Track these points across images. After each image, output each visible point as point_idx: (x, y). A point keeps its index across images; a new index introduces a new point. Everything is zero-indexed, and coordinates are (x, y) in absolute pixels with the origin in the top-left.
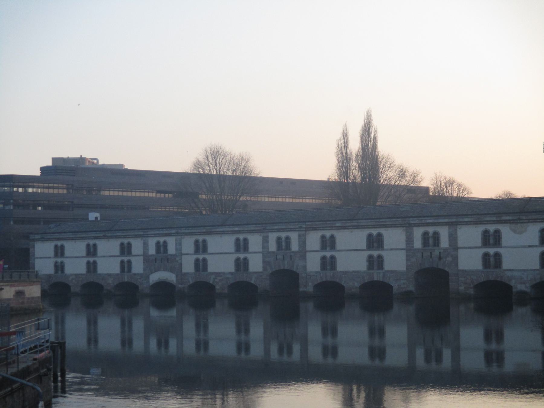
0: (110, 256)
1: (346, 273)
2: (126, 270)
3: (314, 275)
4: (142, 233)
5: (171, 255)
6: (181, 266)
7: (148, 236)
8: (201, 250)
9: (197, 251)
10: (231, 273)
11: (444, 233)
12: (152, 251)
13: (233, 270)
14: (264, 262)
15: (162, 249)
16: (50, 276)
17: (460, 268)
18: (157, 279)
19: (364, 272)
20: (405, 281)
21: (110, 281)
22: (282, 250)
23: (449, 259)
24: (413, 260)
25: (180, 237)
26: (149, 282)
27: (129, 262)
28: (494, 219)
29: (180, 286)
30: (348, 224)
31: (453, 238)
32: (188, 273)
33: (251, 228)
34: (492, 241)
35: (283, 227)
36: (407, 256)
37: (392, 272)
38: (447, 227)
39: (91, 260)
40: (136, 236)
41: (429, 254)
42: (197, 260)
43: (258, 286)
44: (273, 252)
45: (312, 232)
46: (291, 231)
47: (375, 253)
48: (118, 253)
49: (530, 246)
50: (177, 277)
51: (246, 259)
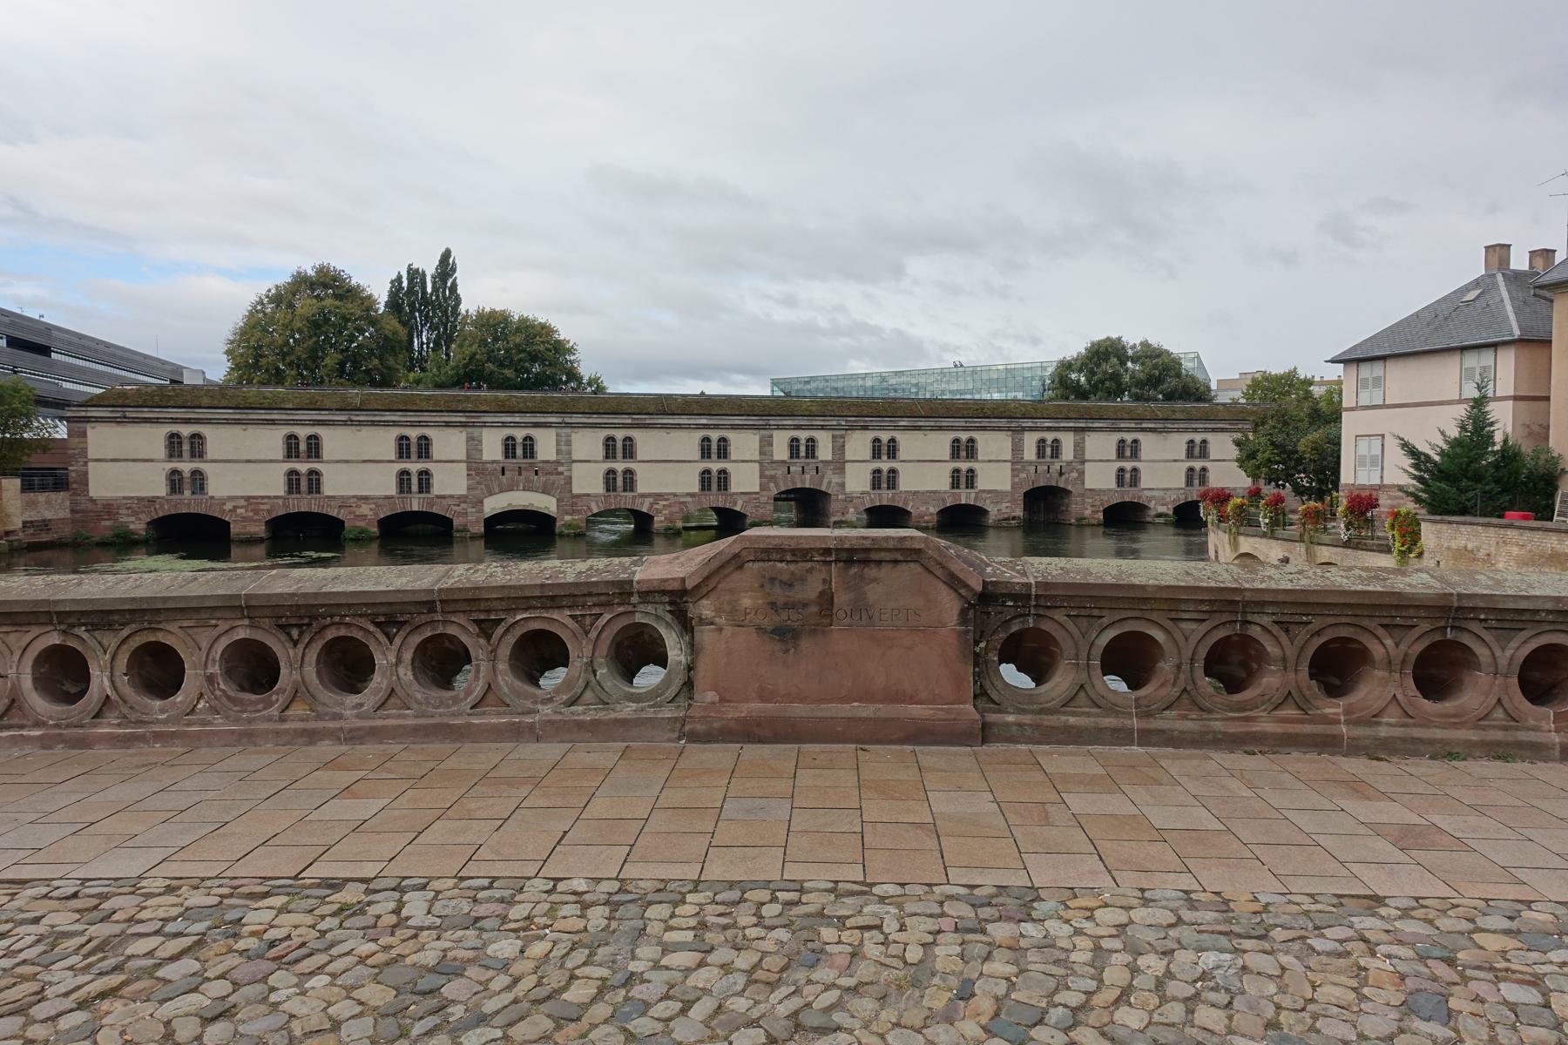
0: (364, 461)
1: (916, 492)
4: (464, 419)
5: (547, 462)
7: (484, 425)
10: (692, 495)
11: (1068, 441)
13: (696, 489)
14: (762, 476)
15: (519, 451)
16: (152, 500)
17: (1088, 485)
19: (945, 492)
20: (1009, 504)
21: (365, 510)
22: (798, 457)
23: (1075, 475)
26: (482, 511)
28: (1133, 425)
29: (568, 518)
30: (920, 424)
31: (1079, 448)
32: (588, 495)
34: (1128, 453)
36: (1013, 470)
37: (989, 492)
40: (448, 425)
41: (1046, 468)
42: (611, 473)
44: (783, 462)
50: (558, 501)
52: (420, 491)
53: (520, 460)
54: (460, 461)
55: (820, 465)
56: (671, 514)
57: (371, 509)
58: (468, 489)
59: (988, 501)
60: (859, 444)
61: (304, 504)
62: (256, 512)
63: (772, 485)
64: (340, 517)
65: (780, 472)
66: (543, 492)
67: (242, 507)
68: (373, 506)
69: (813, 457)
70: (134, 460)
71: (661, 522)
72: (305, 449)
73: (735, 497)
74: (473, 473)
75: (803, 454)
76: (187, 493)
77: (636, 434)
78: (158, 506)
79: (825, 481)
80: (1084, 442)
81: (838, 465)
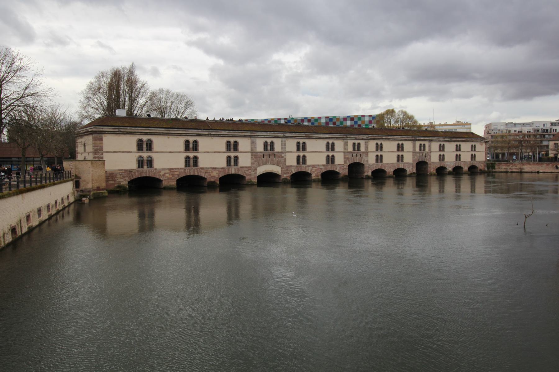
0: (215, 152)
1: (388, 164)
2: (232, 163)
3: (372, 166)
5: (278, 152)
7: (258, 137)
8: (301, 149)
10: (324, 165)
13: (324, 162)
14: (345, 158)
15: (269, 148)
16: (131, 171)
17: (432, 161)
18: (264, 171)
19: (396, 164)
23: (429, 157)
24: (416, 157)
25: (285, 139)
26: (256, 173)
29: (285, 176)
31: (430, 147)
32: (291, 166)
34: (442, 149)
36: (413, 155)
38: (428, 142)
40: (245, 136)
43: (340, 173)
44: (351, 152)
46: (363, 139)
48: (224, 149)
49: (453, 152)
51: (333, 156)
52: (234, 165)
53: (269, 152)
54: (248, 152)
55: (361, 153)
56: (317, 173)
57: (217, 173)
58: (251, 164)
59: (407, 167)
61: (192, 171)
62: (173, 175)
63: (348, 161)
64: (205, 177)
65: (350, 156)
66: (277, 165)
67: (168, 173)
68: (218, 172)
70: (123, 152)
71: (314, 176)
73: (336, 166)
74: (253, 157)
75: (356, 149)
76: (145, 167)
77: (306, 141)
78: (133, 174)
79: (363, 159)
80: (431, 145)
81: (366, 153)
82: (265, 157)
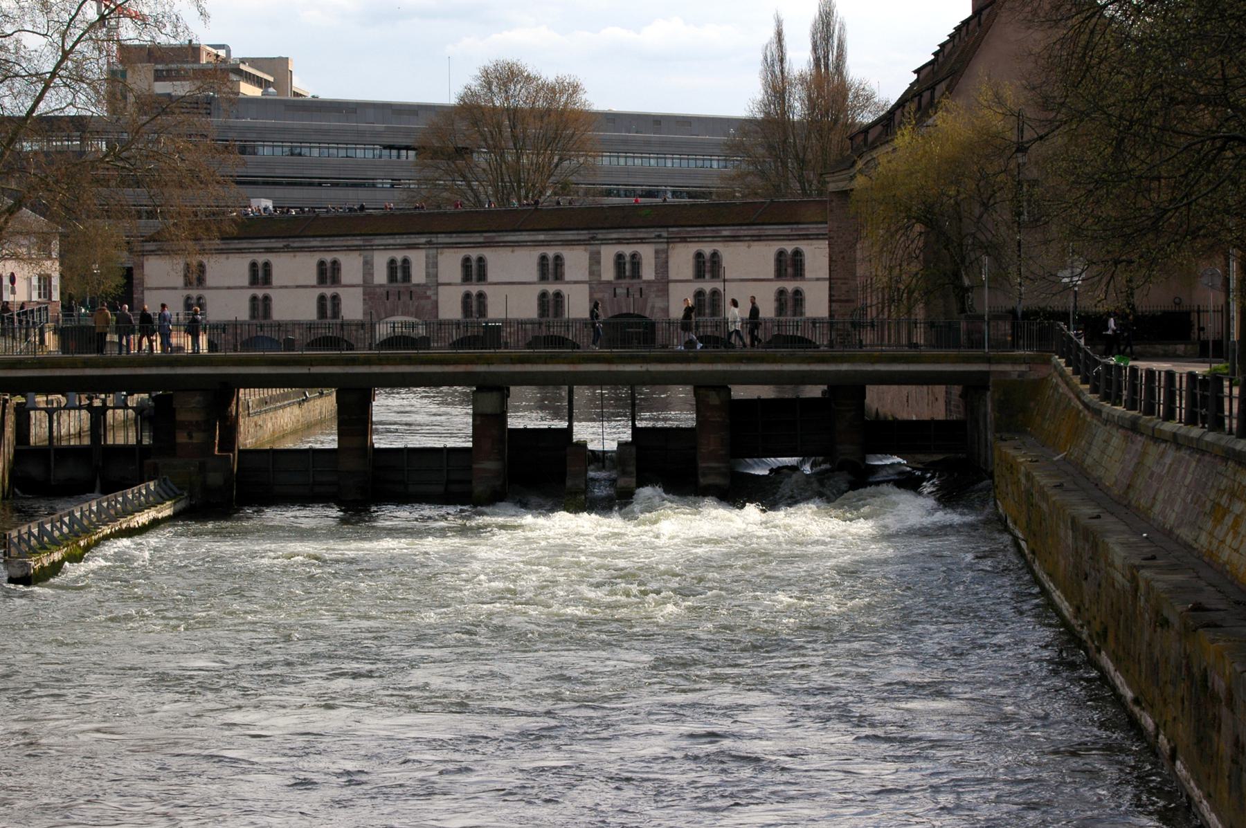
0: (297, 287)
2: (329, 313)
4: (361, 243)
5: (418, 285)
6: (437, 307)
7: (372, 248)
8: (474, 277)
9: (467, 278)
10: (532, 322)
12: (381, 277)
15: (399, 275)
25: (434, 251)
27: (335, 298)
30: (742, 233)
33: (570, 235)
35: (628, 235)
39: (260, 293)
40: (349, 249)
42: (467, 296)
44: (609, 282)
45: (680, 245)
47: (790, 286)
48: (313, 280)
55: (644, 286)
60: (682, 259)
65: (607, 295)
69: (639, 277)
72: (261, 276)
77: (488, 254)
79: (649, 305)
82: (391, 298)
